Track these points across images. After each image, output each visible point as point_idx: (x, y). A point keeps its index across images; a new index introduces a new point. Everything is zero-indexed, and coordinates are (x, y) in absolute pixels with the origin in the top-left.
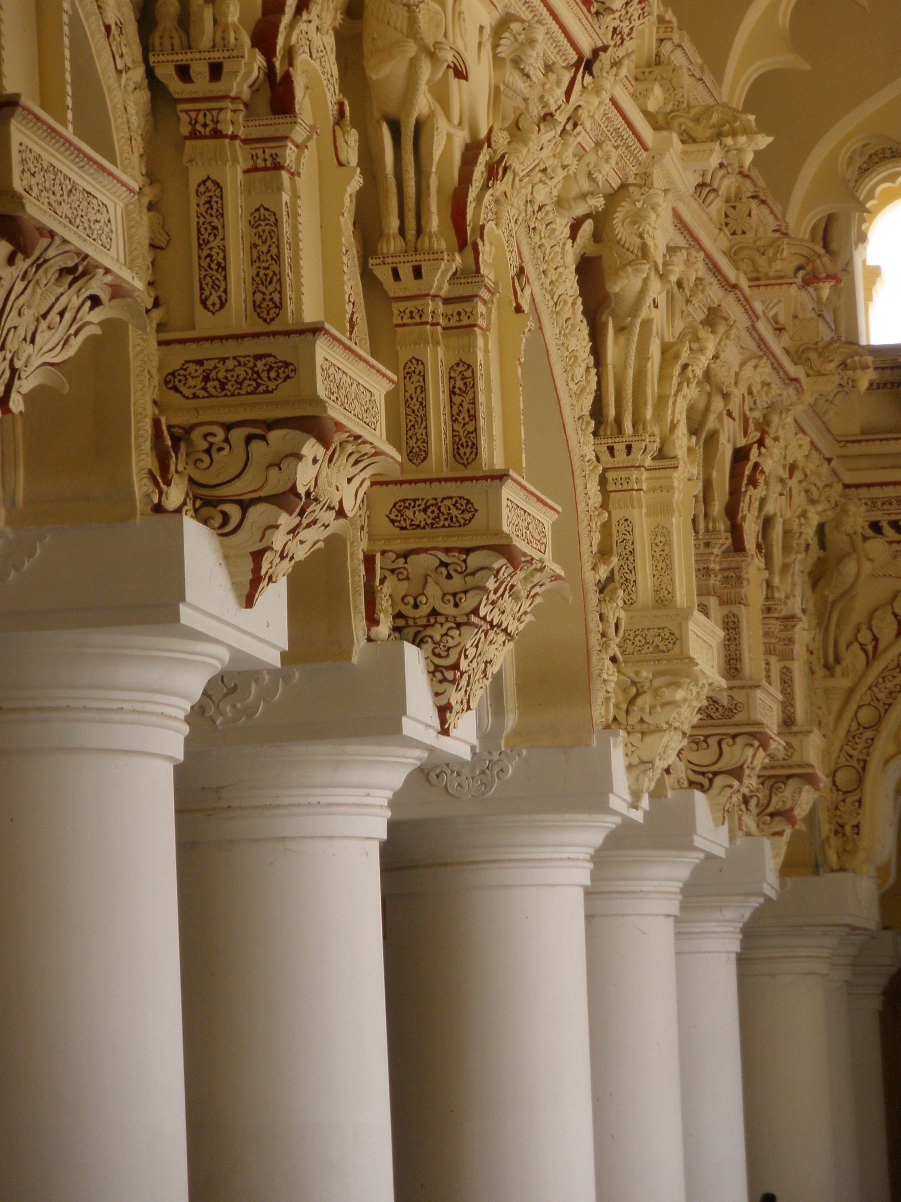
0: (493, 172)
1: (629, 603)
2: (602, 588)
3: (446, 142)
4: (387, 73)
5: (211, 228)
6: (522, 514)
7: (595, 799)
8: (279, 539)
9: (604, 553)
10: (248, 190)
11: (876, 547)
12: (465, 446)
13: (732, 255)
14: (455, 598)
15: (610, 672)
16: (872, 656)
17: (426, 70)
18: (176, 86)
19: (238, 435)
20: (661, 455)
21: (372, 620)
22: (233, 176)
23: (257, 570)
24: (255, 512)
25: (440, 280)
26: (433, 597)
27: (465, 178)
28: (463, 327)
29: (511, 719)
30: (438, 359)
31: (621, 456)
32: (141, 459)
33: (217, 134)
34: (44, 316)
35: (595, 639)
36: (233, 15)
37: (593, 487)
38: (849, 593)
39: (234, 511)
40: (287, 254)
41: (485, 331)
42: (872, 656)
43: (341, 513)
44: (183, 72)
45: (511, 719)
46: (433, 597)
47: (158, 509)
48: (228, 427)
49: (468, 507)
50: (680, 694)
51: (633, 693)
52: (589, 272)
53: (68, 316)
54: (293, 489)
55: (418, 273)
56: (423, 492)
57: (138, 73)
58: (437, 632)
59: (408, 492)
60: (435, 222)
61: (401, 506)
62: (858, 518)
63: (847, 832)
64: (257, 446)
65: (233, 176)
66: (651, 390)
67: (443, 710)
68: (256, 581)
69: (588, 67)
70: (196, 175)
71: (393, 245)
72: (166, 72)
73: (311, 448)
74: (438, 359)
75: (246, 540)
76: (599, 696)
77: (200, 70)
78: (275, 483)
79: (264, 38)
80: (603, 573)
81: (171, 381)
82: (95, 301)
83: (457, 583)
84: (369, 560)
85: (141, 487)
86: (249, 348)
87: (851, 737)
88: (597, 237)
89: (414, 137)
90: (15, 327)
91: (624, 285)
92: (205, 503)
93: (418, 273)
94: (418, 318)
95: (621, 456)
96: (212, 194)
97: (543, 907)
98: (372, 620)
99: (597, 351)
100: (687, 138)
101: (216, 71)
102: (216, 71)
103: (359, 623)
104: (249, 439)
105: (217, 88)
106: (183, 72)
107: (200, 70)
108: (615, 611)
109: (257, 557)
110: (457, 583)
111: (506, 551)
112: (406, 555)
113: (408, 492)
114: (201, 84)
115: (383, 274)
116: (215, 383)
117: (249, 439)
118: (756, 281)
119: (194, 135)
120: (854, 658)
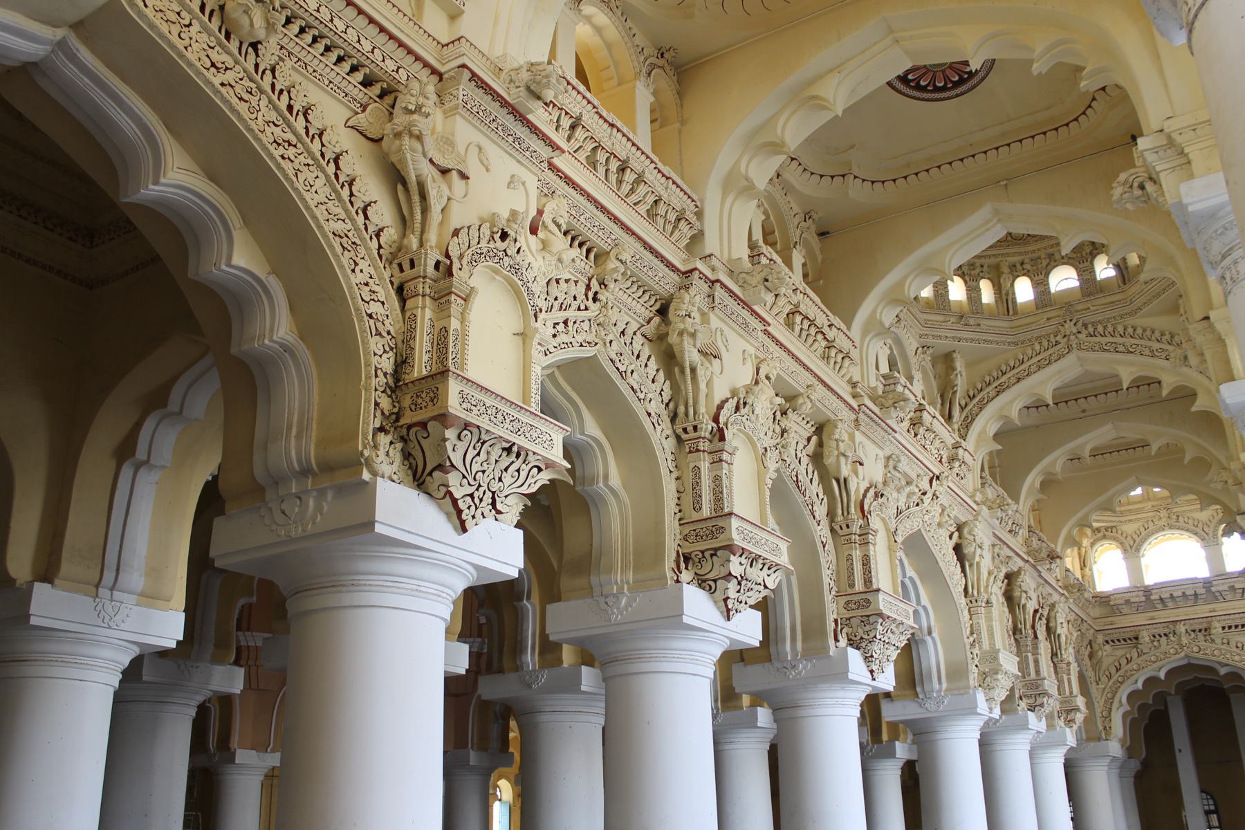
0: (879, 495)
1: (980, 648)
2: (972, 645)
3: (857, 486)
4: (829, 461)
5: (696, 484)
6: (884, 603)
7: (972, 711)
8: (732, 594)
9: (972, 633)
10: (711, 470)
11: (1107, 647)
12: (868, 581)
13: (1028, 553)
14: (867, 633)
15: (976, 670)
16: (1110, 678)
17: (842, 460)
18: (684, 436)
19: (707, 554)
20: (988, 602)
21: (836, 640)
22: (705, 465)
23: (727, 606)
24: (719, 582)
25: (855, 529)
26: (860, 633)
27: (865, 496)
28: (865, 543)
29: (944, 686)
30: (857, 554)
31: (975, 604)
32: (669, 563)
33: (698, 451)
34: (506, 470)
35: (969, 661)
36: (702, 410)
37: (966, 612)
38: (1100, 661)
39: (712, 584)
40: (725, 490)
41: (874, 545)
42: (1110, 678)
43: (765, 587)
44: (685, 430)
45: (944, 686)
46: (860, 633)
47: (678, 581)
48: (703, 552)
49: (868, 601)
50: (999, 677)
51: (984, 675)
52: (958, 549)
53: (523, 474)
54: (730, 574)
55: (848, 526)
56: (855, 598)
57: (669, 432)
58: (863, 645)
59: (849, 598)
60: (853, 510)
61: (847, 603)
62: (1100, 638)
63: (1107, 730)
64: (715, 558)
65: (705, 465)
66: (983, 584)
67: (872, 672)
68: (728, 610)
69: (938, 478)
70: (692, 465)
71: (840, 518)
72: (679, 431)
73: (734, 560)
74: (857, 554)
75: (719, 595)
76: (971, 677)
77: (690, 429)
78: (724, 573)
79: (716, 419)
80: (971, 639)
81: (685, 538)
82: (540, 470)
83: (868, 628)
84: (836, 621)
85: (669, 574)
86: (709, 523)
87: (1106, 702)
88: (960, 537)
89: (844, 484)
90: (484, 472)
91: (968, 550)
92: (702, 582)
93: (848, 526)
94: (849, 542)
95: (975, 604)
96: (697, 470)
97: (1014, 754)
98: (836, 640)
99: (963, 571)
100: (990, 508)
101: (695, 428)
102: (695, 428)
103: (831, 641)
104: (712, 555)
105: (696, 435)
106: (685, 430)
107: (690, 429)
108: (976, 651)
109: (725, 600)
110: (868, 628)
111: (880, 615)
112: (849, 619)
113: (849, 598)
114: (692, 435)
115: (837, 528)
116: (699, 537)
117: (712, 555)
118: (1036, 560)
119: (690, 452)
120: (1104, 679)
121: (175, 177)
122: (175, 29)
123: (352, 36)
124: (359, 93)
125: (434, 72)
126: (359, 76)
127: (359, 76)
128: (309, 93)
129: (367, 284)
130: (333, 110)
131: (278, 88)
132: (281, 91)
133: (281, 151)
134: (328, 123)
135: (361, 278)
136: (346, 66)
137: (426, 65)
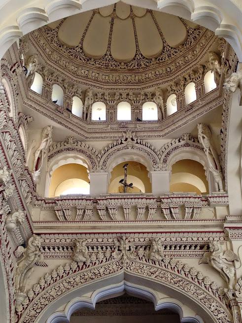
121: (162, 301)
122: (139, 271)
123: (190, 240)
124: (200, 252)
125: (220, 232)
126: (198, 248)
127: (198, 248)
128: (184, 261)
129: (216, 309)
130: (192, 262)
131: (173, 267)
132: (174, 268)
133: (178, 284)
134: (191, 266)
135: (213, 309)
136: (193, 248)
137: (217, 232)
